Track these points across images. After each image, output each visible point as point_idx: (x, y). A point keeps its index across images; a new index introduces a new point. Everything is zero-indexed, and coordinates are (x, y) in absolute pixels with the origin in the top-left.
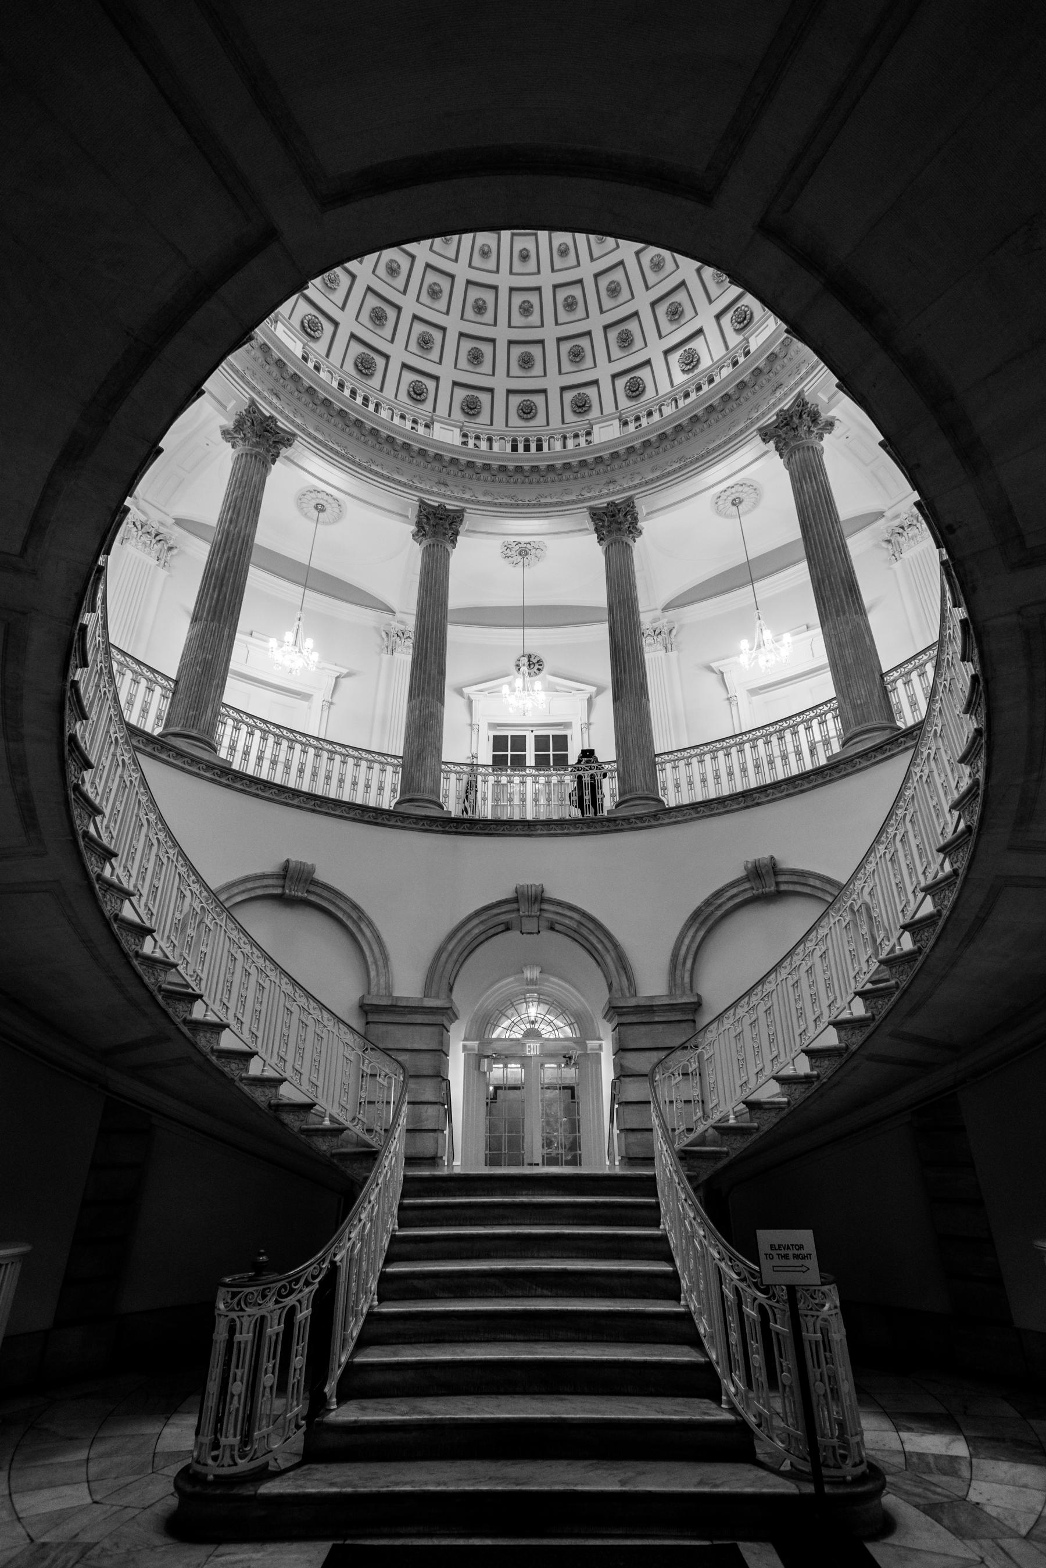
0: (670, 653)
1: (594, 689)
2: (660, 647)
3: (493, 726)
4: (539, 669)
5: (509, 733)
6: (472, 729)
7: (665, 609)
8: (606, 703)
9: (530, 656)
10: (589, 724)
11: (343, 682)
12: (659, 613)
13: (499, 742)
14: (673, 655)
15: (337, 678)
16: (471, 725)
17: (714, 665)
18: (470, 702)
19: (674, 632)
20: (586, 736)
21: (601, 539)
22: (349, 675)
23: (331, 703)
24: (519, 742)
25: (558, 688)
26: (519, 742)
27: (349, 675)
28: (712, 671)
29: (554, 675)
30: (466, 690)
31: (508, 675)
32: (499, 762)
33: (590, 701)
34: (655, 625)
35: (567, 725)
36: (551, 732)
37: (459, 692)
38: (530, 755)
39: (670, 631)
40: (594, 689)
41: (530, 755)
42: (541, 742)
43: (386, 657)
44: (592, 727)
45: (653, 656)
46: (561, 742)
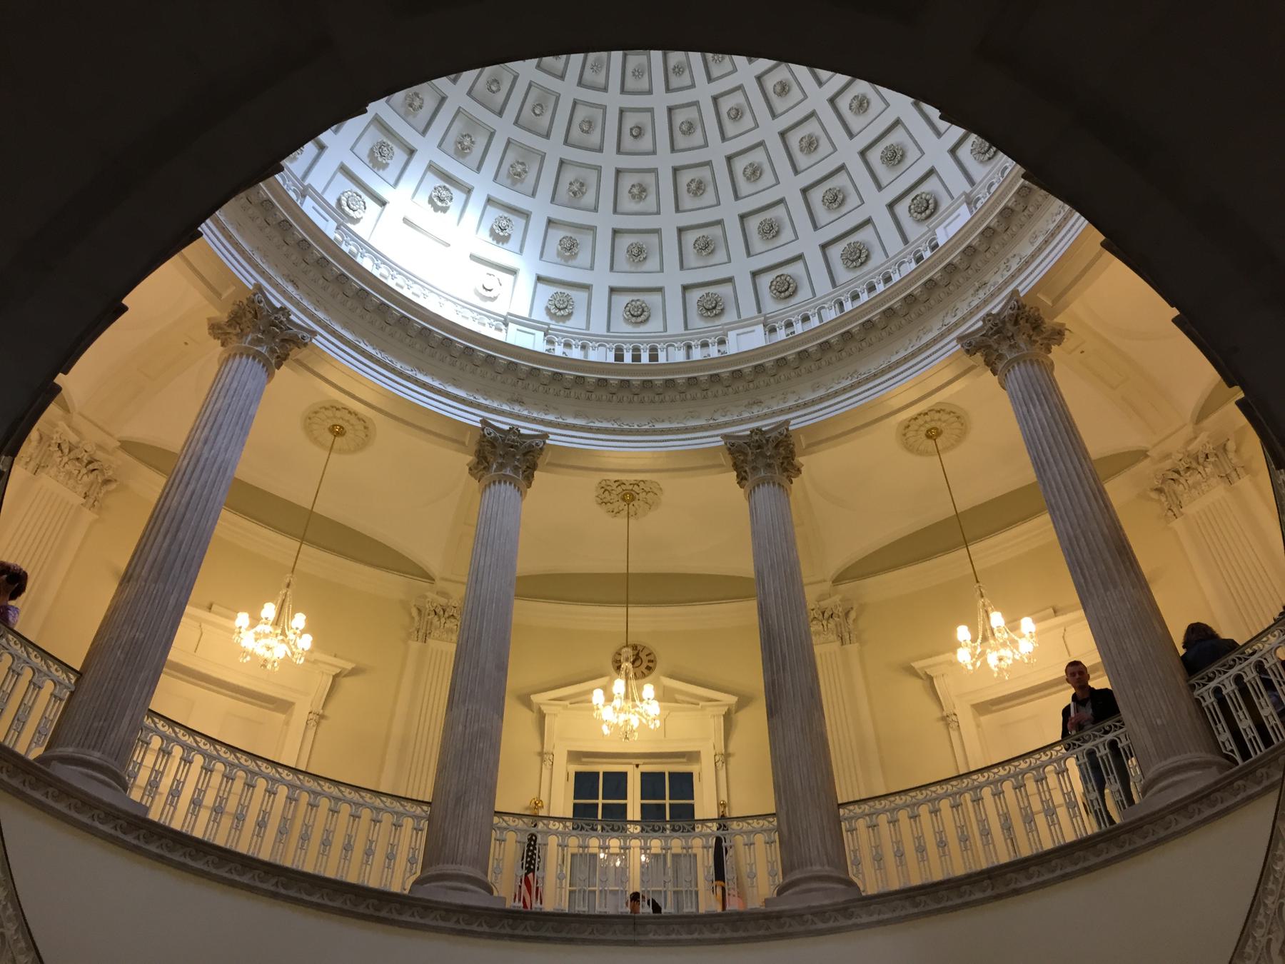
0: (848, 646)
1: (733, 699)
2: (833, 637)
3: (575, 756)
4: (649, 668)
5: (602, 768)
6: (543, 761)
7: (838, 580)
8: (755, 721)
9: (635, 647)
10: (727, 756)
11: (346, 683)
12: (827, 586)
13: (584, 783)
14: (853, 648)
15: (336, 677)
16: (541, 754)
17: (917, 665)
18: (542, 717)
19: (853, 615)
20: (722, 774)
21: (742, 479)
22: (354, 672)
23: (322, 717)
24: (617, 783)
25: (678, 697)
26: (617, 783)
27: (354, 672)
28: (913, 673)
29: (672, 676)
30: (536, 698)
31: (602, 676)
32: (583, 814)
33: (728, 718)
34: (824, 604)
35: (693, 756)
36: (666, 768)
37: (525, 700)
38: (634, 804)
39: (847, 614)
40: (733, 699)
41: (634, 804)
42: (651, 783)
43: (415, 645)
44: (731, 760)
45: (825, 650)
46: (684, 783)
